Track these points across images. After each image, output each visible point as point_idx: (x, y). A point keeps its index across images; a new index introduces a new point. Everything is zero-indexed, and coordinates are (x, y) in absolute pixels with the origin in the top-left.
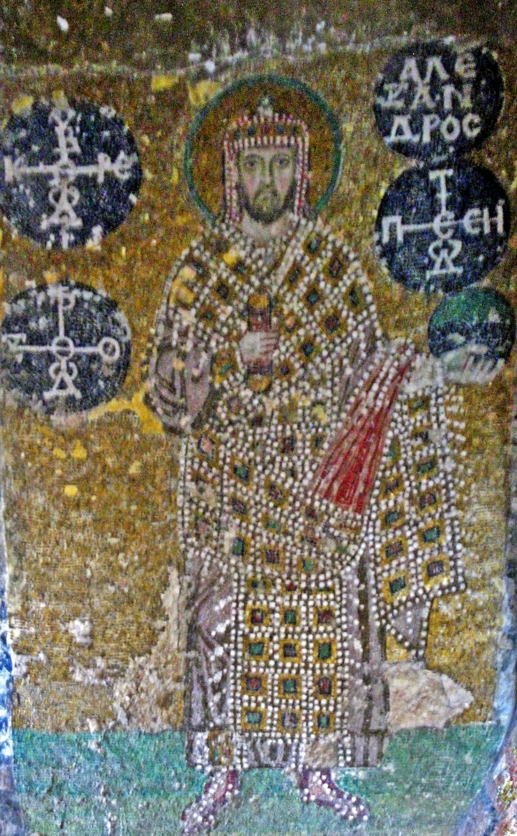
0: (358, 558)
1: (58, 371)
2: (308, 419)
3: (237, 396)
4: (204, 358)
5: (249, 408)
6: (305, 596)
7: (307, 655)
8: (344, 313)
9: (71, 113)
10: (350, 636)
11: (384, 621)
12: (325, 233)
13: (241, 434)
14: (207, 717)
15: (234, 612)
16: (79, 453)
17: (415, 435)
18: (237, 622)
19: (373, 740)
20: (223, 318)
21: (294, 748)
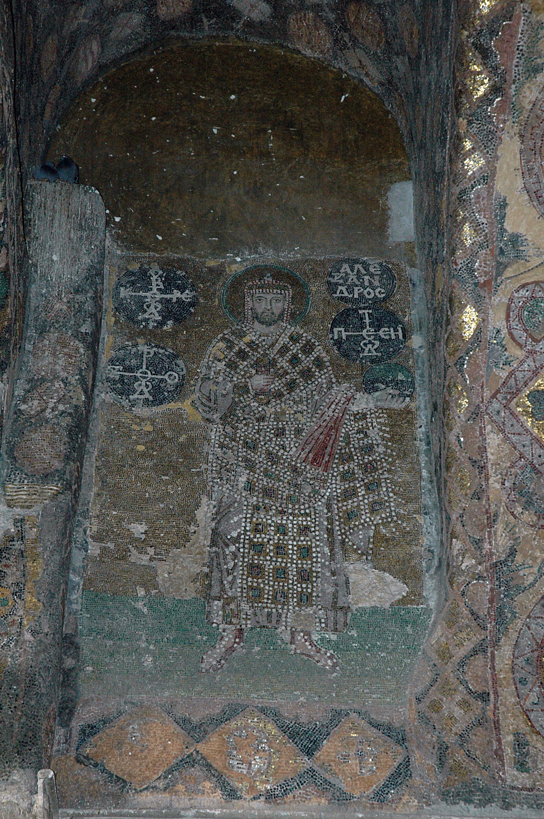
0: (326, 497)
1: (140, 385)
2: (292, 420)
3: (249, 405)
4: (229, 386)
5: (256, 412)
6: (291, 518)
7: (293, 554)
8: (313, 370)
9: (161, 272)
10: (321, 544)
11: (344, 537)
12: (301, 333)
13: (251, 425)
14: (223, 590)
15: (243, 524)
17: (358, 432)
18: (245, 531)
19: (340, 614)
20: (241, 367)
21: (284, 616)
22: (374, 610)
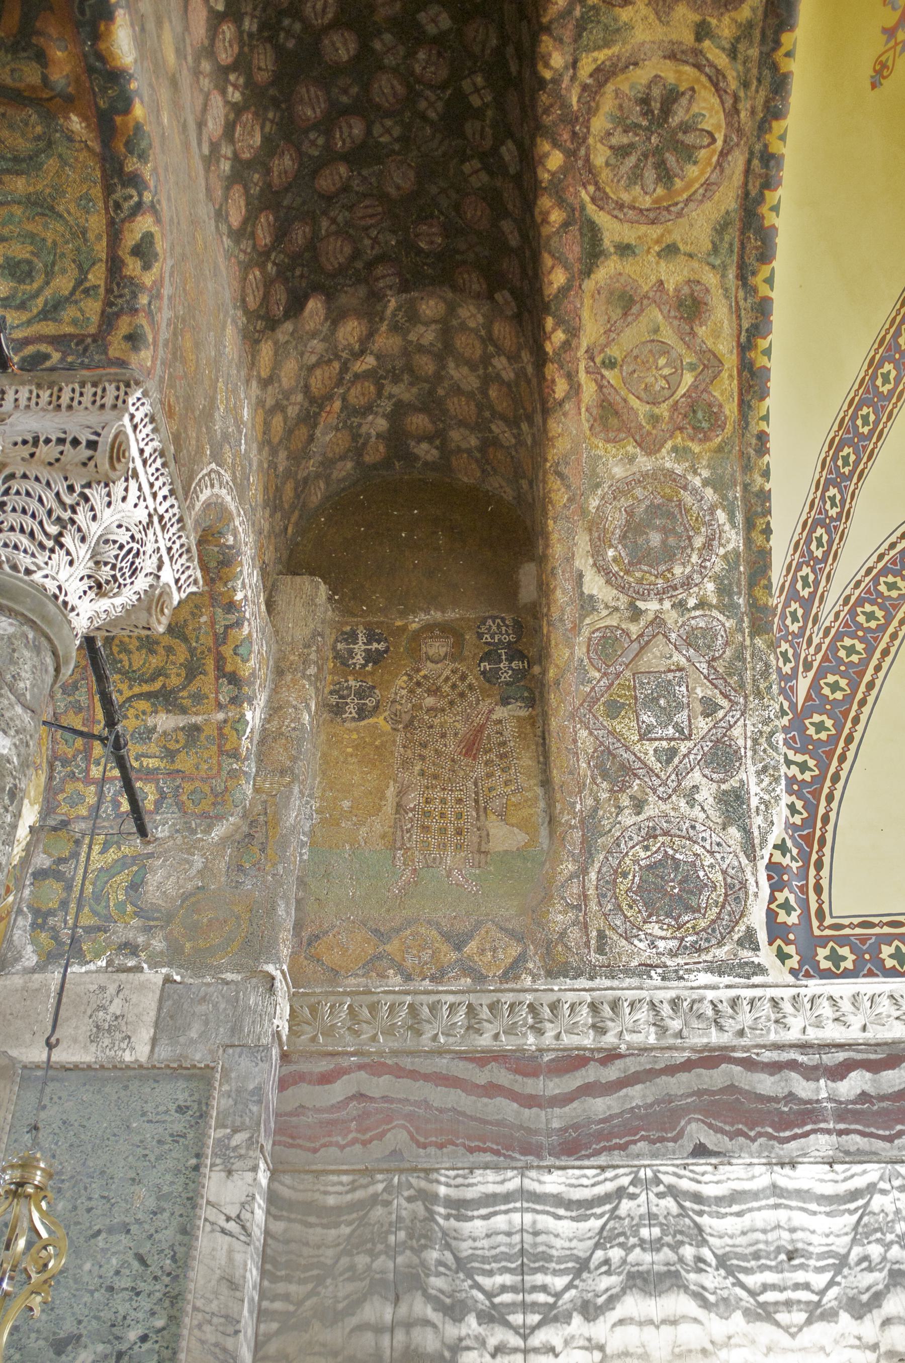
14: (403, 844)
16: (355, 736)
17: (497, 733)
22: (506, 851)
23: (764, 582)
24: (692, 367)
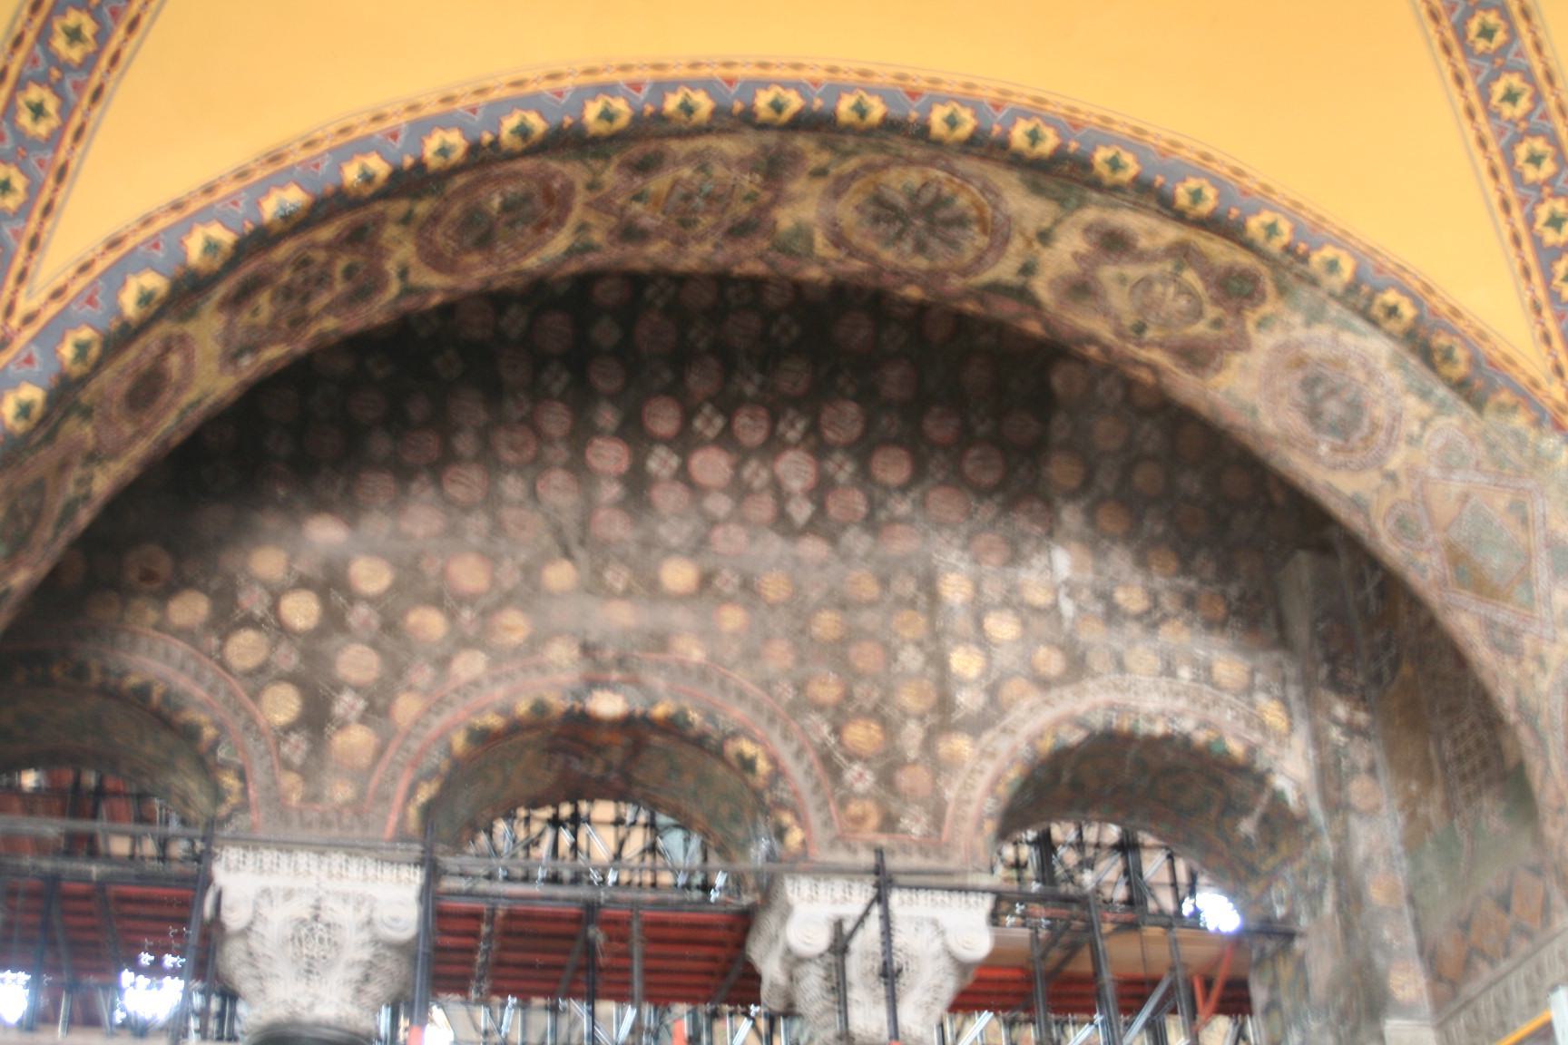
23: (1438, 358)
24: (1179, 267)
